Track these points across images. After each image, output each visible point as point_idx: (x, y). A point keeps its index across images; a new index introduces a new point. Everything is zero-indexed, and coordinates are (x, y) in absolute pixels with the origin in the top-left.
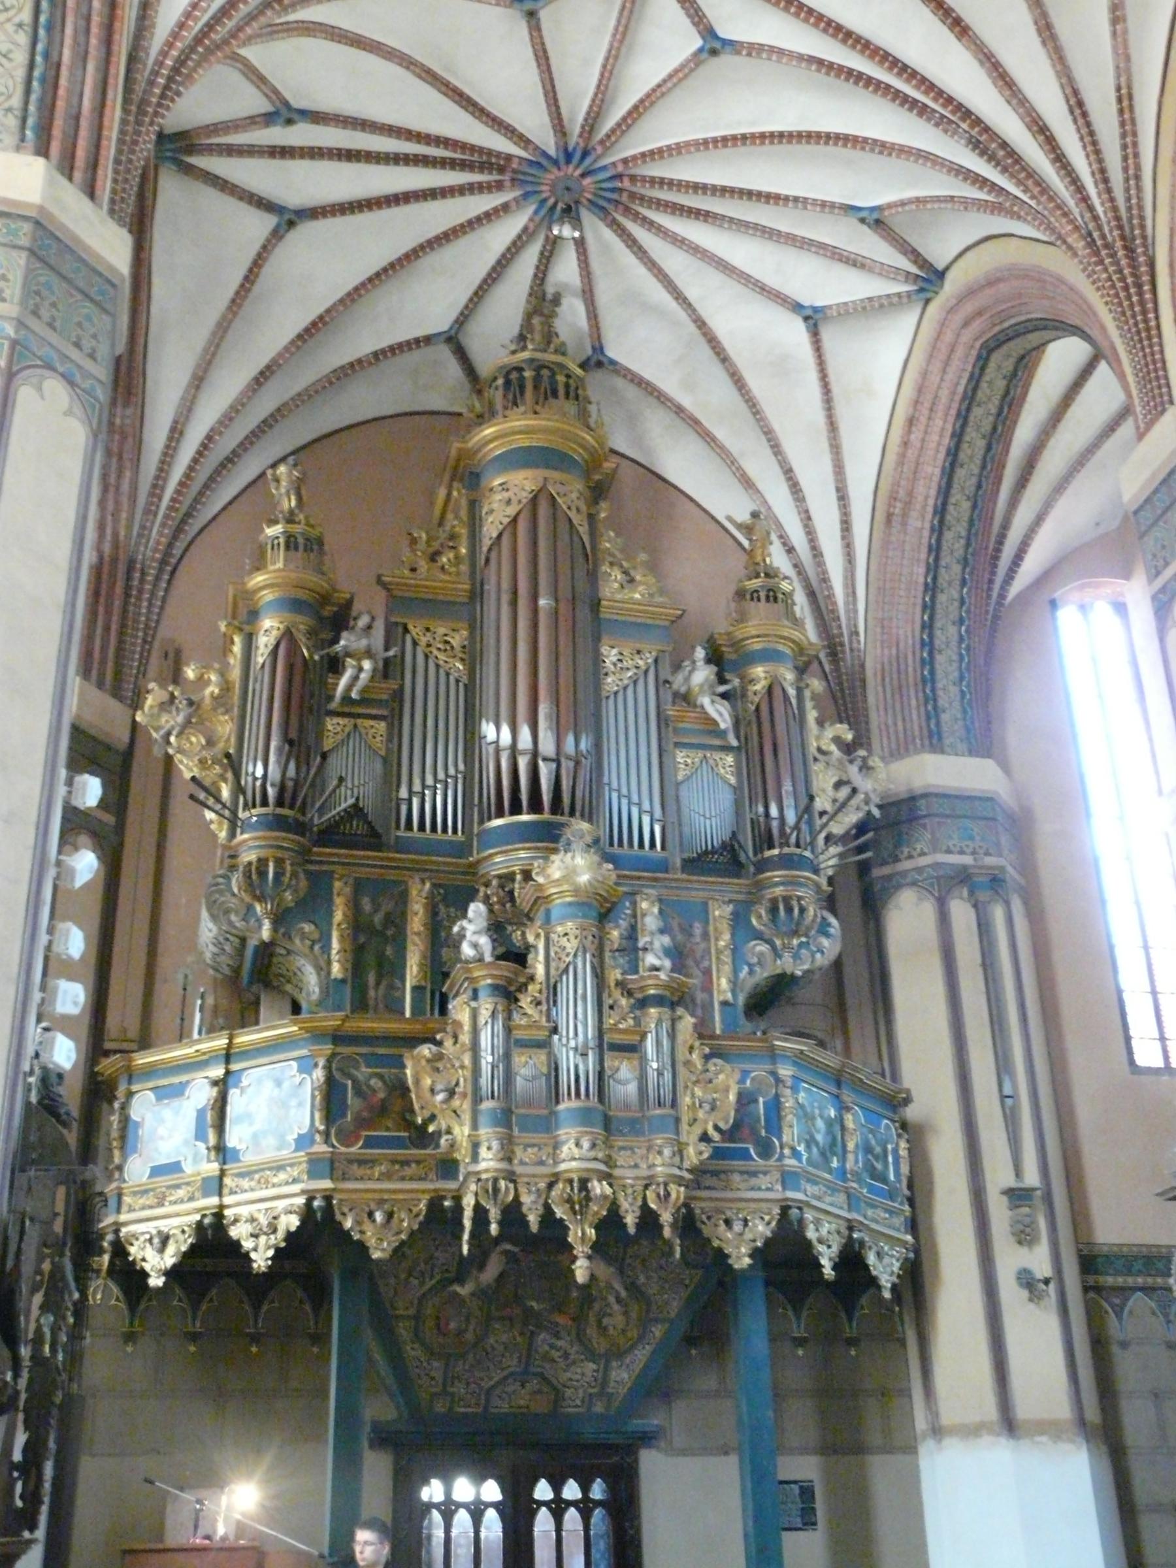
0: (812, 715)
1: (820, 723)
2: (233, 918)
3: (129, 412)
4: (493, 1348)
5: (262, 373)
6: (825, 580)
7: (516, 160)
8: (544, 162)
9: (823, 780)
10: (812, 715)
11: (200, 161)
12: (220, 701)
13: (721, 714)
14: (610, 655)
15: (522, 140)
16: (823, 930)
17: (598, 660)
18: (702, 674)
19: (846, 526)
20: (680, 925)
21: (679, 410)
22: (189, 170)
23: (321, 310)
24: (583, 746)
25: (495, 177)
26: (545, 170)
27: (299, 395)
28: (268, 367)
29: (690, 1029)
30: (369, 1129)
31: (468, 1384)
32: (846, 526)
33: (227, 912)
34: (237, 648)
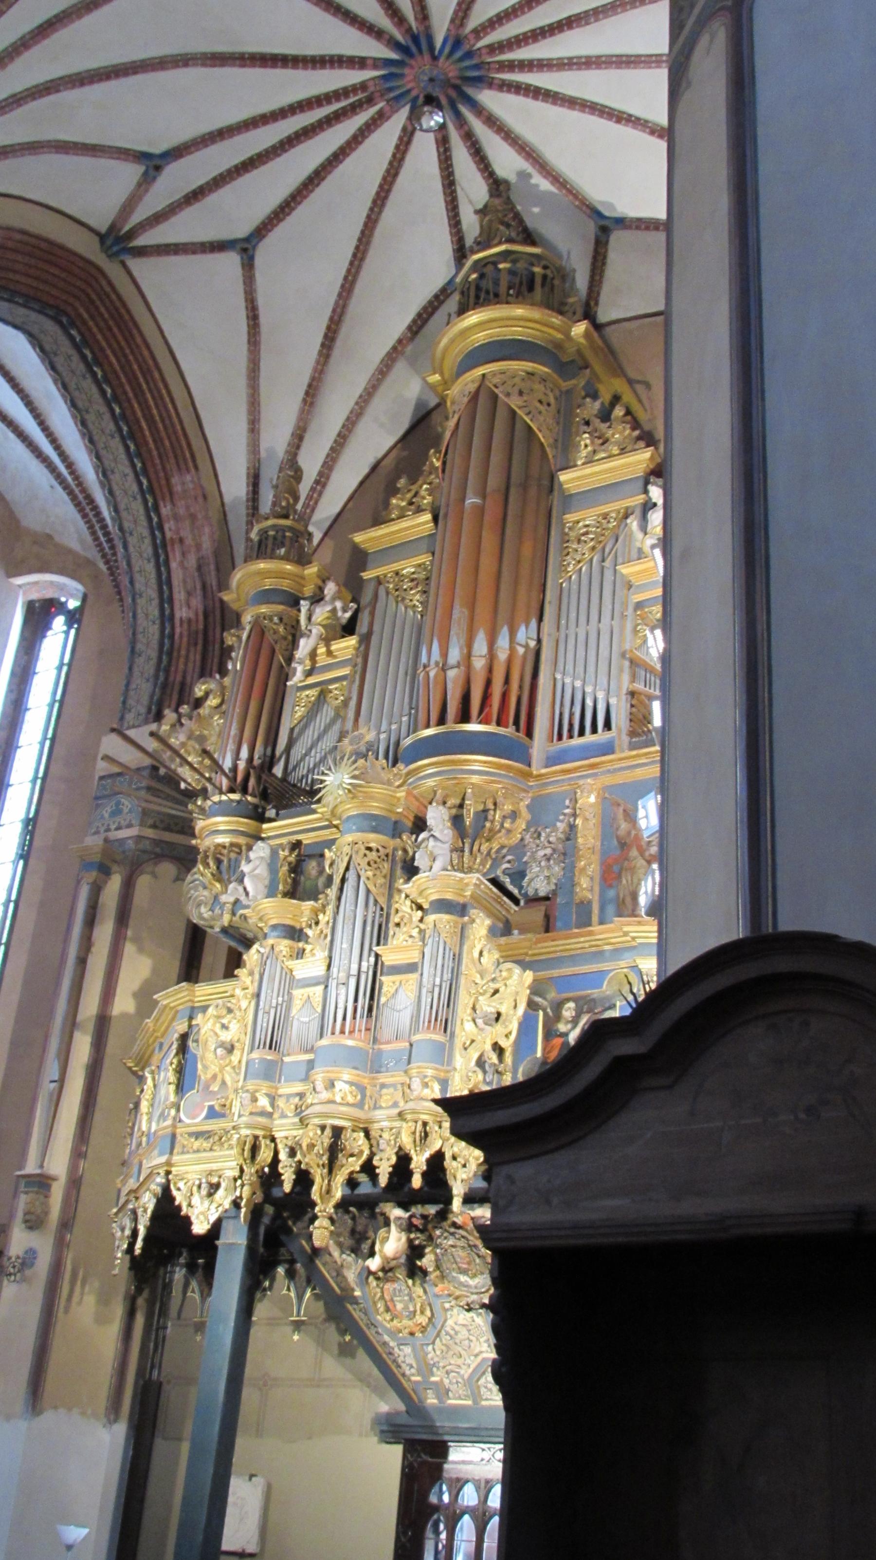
2: (203, 909)
3: (188, 478)
4: (456, 1333)
5: (307, 393)
7: (371, 83)
8: (394, 70)
11: (141, 241)
15: (360, 63)
20: (625, 811)
22: (142, 252)
23: (328, 313)
25: (372, 111)
26: (401, 76)
27: (361, 396)
28: (310, 386)
29: (483, 932)
30: (209, 1101)
31: (448, 1373)
33: (199, 905)
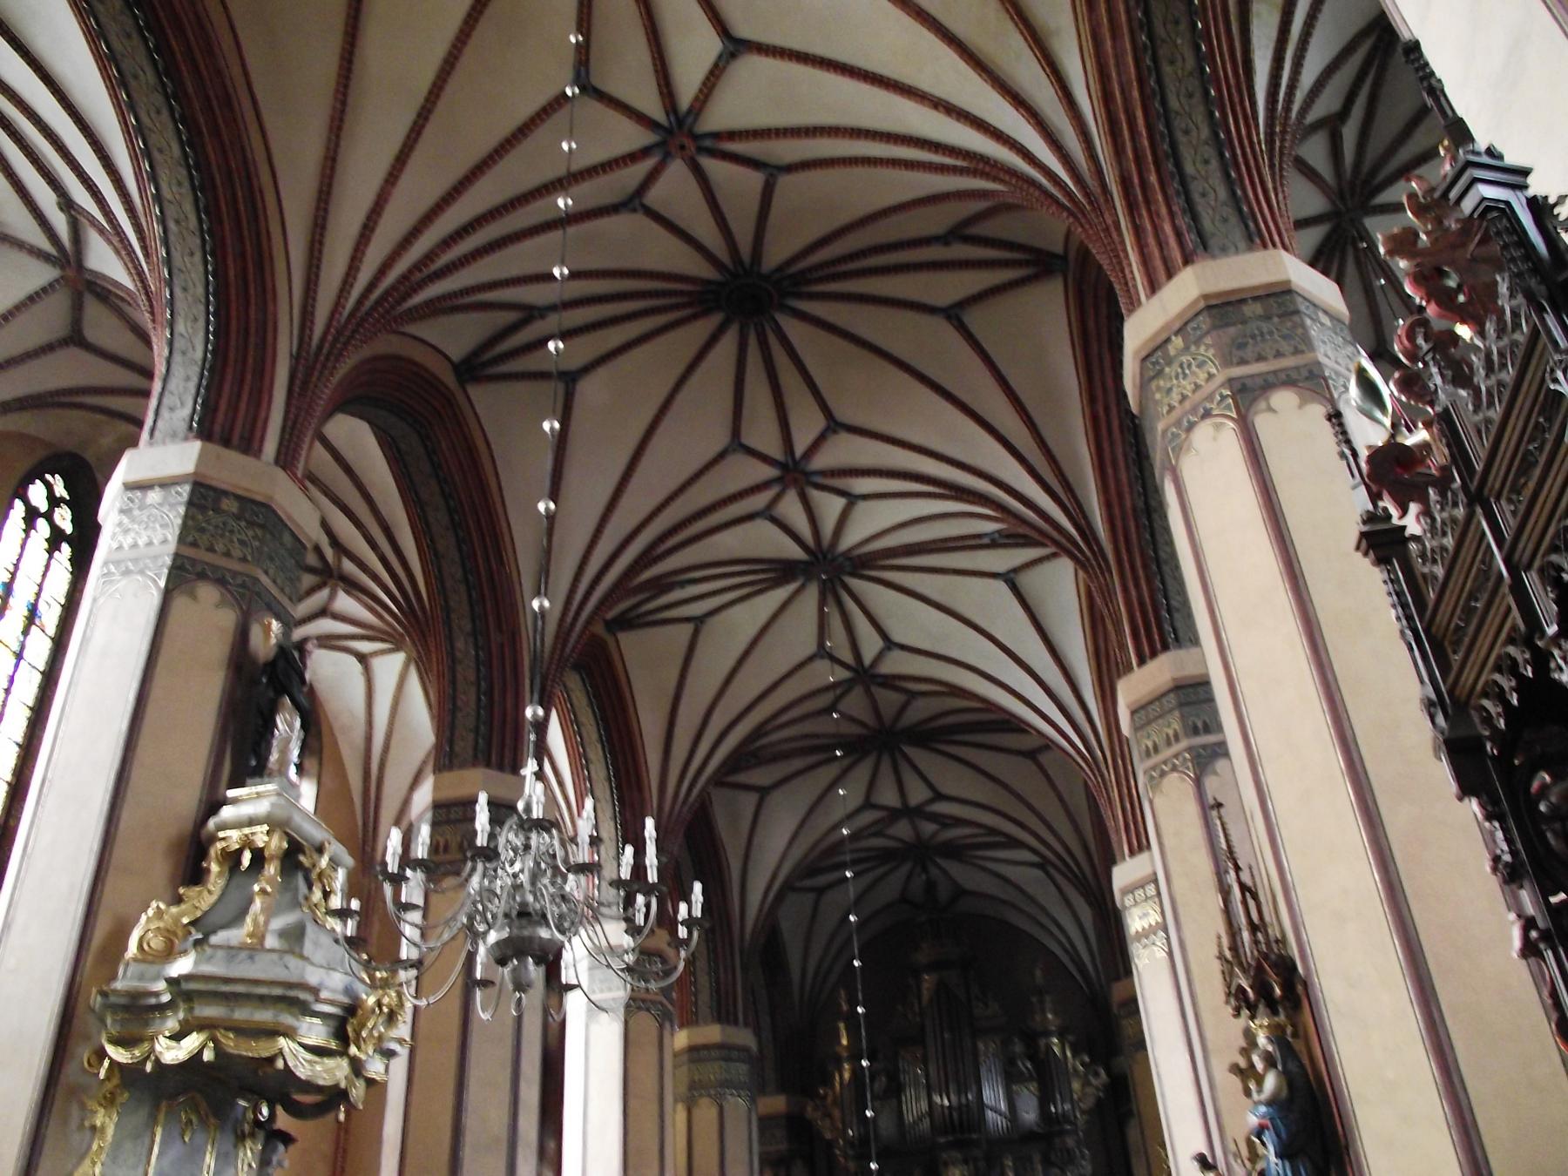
0: (1069, 1054)
1: (1074, 1056)
6: (1084, 964)
9: (1076, 1085)
10: (1069, 1054)
12: (835, 1102)
13: (1026, 1066)
14: (981, 1046)
16: (1083, 1157)
17: (975, 1047)
18: (1018, 1048)
19: (1086, 938)
21: (1004, 902)
24: (970, 1097)
32: (1086, 938)
34: (837, 1078)
